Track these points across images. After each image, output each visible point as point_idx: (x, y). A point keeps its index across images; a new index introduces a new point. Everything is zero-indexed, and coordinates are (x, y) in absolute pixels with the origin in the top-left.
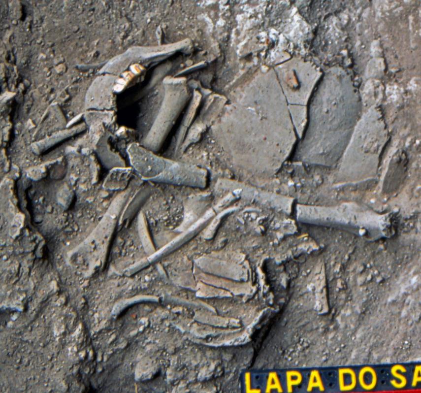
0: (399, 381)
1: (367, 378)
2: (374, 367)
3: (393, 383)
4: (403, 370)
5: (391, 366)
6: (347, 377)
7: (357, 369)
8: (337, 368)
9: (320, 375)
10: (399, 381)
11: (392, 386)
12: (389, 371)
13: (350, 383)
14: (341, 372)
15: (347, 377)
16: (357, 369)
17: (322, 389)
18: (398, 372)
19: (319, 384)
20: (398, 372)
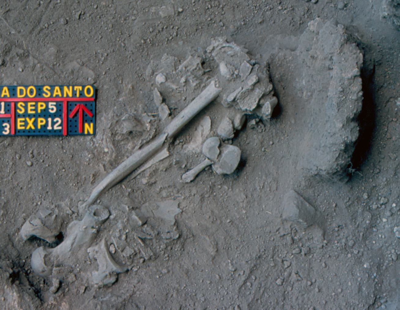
0: (47, 94)
1: (31, 92)
2: (35, 86)
3: (44, 95)
4: (49, 88)
5: (44, 86)
6: (21, 91)
7: (26, 87)
8: (16, 87)
9: (9, 90)
10: (47, 94)
11: (43, 97)
12: (42, 89)
13: (23, 94)
14: (19, 88)
15: (21, 91)
16: (26, 87)
17: (8, 96)
18: (47, 89)
19: (7, 94)
20: (47, 89)
